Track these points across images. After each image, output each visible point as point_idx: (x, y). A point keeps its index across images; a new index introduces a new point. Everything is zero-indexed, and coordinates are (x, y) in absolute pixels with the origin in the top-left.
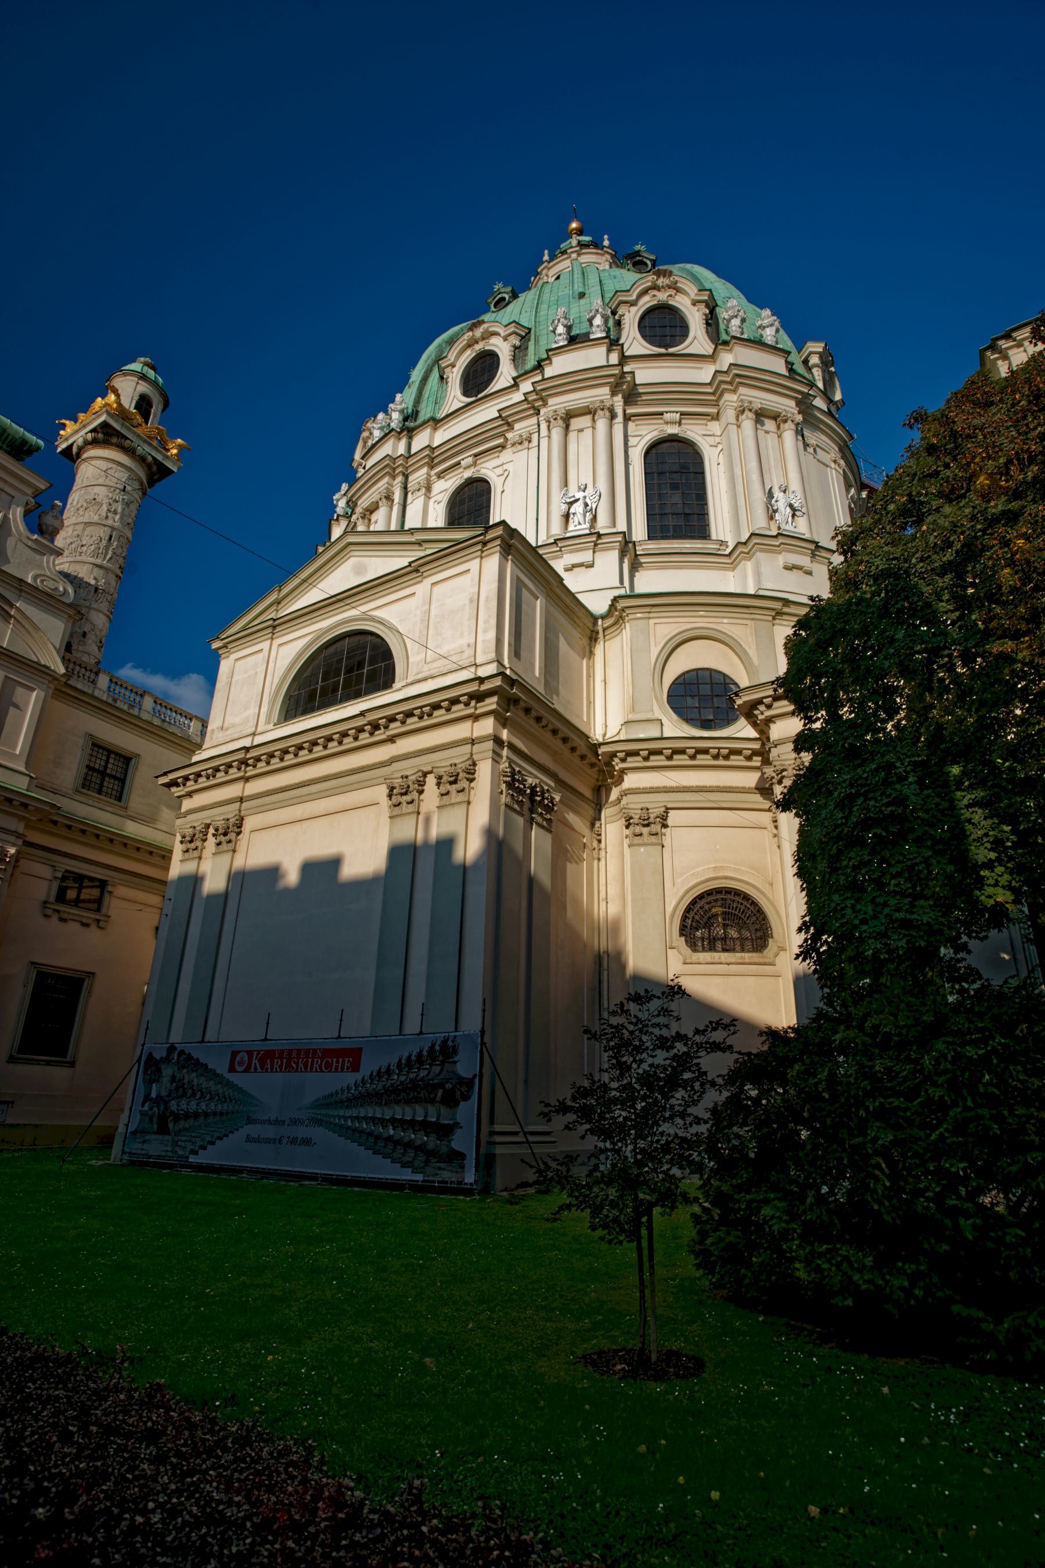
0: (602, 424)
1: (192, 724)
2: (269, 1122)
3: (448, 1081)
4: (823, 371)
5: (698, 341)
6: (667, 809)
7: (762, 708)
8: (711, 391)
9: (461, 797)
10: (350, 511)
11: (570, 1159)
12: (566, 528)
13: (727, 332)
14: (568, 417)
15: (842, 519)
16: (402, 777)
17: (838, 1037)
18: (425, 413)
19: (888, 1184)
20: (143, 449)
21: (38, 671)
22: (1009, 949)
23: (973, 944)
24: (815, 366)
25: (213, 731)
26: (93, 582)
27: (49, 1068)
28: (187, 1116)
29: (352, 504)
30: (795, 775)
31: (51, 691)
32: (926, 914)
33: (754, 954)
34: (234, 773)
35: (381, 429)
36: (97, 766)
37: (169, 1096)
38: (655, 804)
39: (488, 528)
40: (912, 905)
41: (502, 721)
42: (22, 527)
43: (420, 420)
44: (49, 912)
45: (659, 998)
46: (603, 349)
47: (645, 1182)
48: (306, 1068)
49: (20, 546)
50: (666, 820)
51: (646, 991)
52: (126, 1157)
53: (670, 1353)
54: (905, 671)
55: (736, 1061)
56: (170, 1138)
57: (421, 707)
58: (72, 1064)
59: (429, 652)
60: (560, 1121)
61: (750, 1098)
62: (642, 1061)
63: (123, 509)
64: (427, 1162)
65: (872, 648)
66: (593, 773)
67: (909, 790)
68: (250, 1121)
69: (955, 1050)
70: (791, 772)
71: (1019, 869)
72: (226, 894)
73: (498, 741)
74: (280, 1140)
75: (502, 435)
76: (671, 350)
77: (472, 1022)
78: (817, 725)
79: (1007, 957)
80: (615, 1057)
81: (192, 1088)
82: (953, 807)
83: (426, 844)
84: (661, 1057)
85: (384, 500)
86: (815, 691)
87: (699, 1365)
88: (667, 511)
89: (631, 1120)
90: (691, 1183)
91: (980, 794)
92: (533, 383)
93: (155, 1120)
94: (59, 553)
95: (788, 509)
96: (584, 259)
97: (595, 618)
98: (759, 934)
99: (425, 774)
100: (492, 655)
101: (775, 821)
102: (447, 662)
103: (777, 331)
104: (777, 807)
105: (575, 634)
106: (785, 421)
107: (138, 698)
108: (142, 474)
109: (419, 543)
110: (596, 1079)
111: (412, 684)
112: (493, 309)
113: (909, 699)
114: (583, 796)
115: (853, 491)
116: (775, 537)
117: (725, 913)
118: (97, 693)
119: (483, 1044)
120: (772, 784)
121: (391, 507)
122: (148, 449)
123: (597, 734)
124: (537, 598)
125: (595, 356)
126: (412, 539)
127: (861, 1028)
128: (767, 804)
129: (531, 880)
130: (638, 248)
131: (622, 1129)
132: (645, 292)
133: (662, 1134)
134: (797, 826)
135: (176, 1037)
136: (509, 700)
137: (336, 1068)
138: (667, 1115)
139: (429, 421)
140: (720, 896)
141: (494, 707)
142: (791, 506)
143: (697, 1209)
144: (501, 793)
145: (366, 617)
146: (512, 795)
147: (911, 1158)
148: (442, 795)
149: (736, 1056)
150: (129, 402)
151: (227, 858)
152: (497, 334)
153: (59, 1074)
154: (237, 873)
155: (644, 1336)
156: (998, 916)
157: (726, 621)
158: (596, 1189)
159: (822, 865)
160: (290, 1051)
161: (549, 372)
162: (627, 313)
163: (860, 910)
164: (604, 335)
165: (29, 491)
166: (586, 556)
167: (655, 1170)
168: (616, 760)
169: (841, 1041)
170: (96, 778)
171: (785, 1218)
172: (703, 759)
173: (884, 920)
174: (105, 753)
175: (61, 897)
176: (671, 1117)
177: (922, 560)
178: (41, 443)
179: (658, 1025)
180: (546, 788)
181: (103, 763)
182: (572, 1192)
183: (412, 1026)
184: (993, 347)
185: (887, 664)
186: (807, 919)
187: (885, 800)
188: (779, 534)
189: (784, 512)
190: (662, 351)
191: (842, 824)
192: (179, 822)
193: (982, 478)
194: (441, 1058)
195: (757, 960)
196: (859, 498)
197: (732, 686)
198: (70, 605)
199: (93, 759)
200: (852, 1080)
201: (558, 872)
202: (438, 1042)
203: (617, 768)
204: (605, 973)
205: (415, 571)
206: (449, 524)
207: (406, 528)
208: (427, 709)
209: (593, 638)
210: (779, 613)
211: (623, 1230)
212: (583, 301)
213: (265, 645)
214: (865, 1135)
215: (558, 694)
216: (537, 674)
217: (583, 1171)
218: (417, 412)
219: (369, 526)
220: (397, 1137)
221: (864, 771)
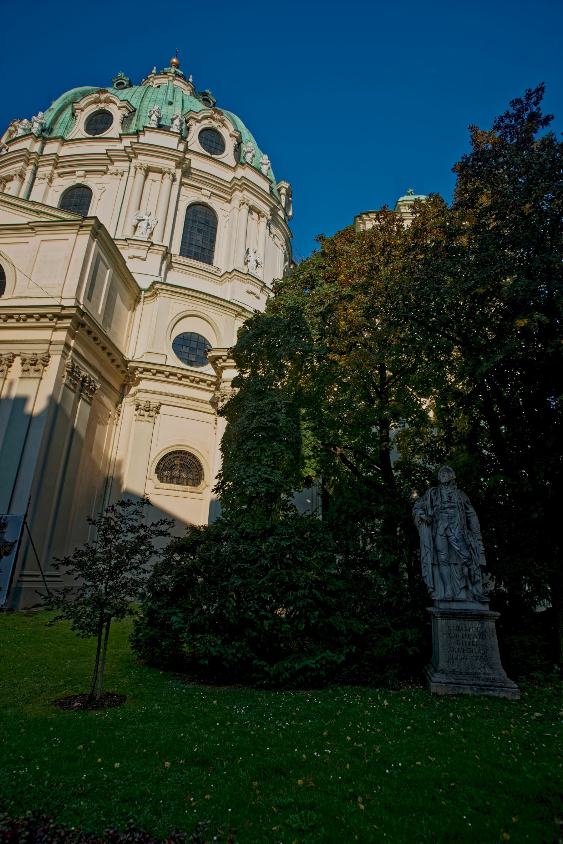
4: (286, 199)
5: (228, 156)
6: (161, 404)
7: (221, 361)
8: (230, 186)
9: (36, 375)
11: (67, 590)
12: (134, 234)
13: (244, 159)
15: (279, 275)
17: (224, 532)
19: (235, 605)
22: (311, 497)
23: (296, 494)
24: (283, 194)
30: (230, 398)
32: (277, 477)
33: (193, 487)
38: (155, 400)
39: (85, 218)
40: (272, 472)
43: (53, 135)
45: (135, 505)
46: (176, 140)
47: (110, 604)
50: (159, 410)
51: (129, 500)
53: (108, 694)
54: (292, 358)
55: (172, 541)
57: (19, 314)
60: (64, 569)
61: (176, 561)
62: (118, 538)
65: (279, 343)
66: (123, 376)
67: (281, 416)
69: (276, 542)
70: (228, 397)
71: (322, 461)
73: (67, 346)
75: (106, 165)
76: (213, 156)
78: (246, 376)
79: (309, 501)
80: (104, 535)
82: (299, 428)
83: (7, 398)
84: (130, 537)
85: (18, 177)
86: (248, 358)
87: (123, 698)
88: (193, 243)
89: (107, 570)
90: (135, 603)
91: (312, 425)
92: (131, 142)
95: (255, 262)
96: (176, 83)
97: (140, 290)
98: (197, 477)
99: (14, 356)
100: (73, 294)
101: (216, 420)
103: (269, 169)
104: (218, 414)
105: (127, 296)
106: (263, 217)
109: (38, 212)
110: (90, 546)
113: (291, 373)
115: (287, 263)
116: (246, 274)
117: (181, 464)
119: (25, 522)
120: (218, 401)
121: (22, 183)
123: (128, 356)
124: (108, 269)
125: (171, 142)
127: (236, 529)
128: (213, 411)
129: (73, 431)
130: (207, 91)
131: (102, 575)
132: (206, 118)
133: (123, 578)
134: (226, 425)
136: (79, 323)
138: (128, 568)
139: (59, 138)
140: (180, 455)
141: (69, 325)
142: (256, 261)
143: (137, 619)
144: (64, 377)
146: (70, 380)
147: (248, 592)
148: (24, 371)
149: (173, 539)
152: (116, 104)
155: (94, 687)
156: (308, 482)
157: (211, 311)
158: (79, 608)
159: (234, 446)
161: (142, 139)
162: (194, 125)
163: (247, 471)
164: (178, 131)
167: (116, 597)
168: (137, 372)
169: (225, 536)
171: (182, 622)
172: (185, 381)
173: (257, 478)
176: (130, 569)
177: (310, 307)
179: (132, 519)
180: (92, 379)
182: (65, 609)
184: (360, 217)
185: (284, 353)
186: (221, 472)
187: (269, 419)
188: (248, 274)
189: (252, 264)
190: (209, 154)
191: (247, 427)
193: (342, 276)
195: (193, 490)
196: (290, 268)
197: (208, 346)
200: (227, 554)
201: (91, 428)
203: (137, 376)
204: (109, 488)
206: (60, 207)
207: (30, 200)
209: (137, 301)
210: (239, 314)
211: (92, 630)
212: (170, 107)
214: (228, 581)
215: (110, 327)
216: (99, 312)
217: (75, 597)
219: (3, 189)
221: (262, 403)
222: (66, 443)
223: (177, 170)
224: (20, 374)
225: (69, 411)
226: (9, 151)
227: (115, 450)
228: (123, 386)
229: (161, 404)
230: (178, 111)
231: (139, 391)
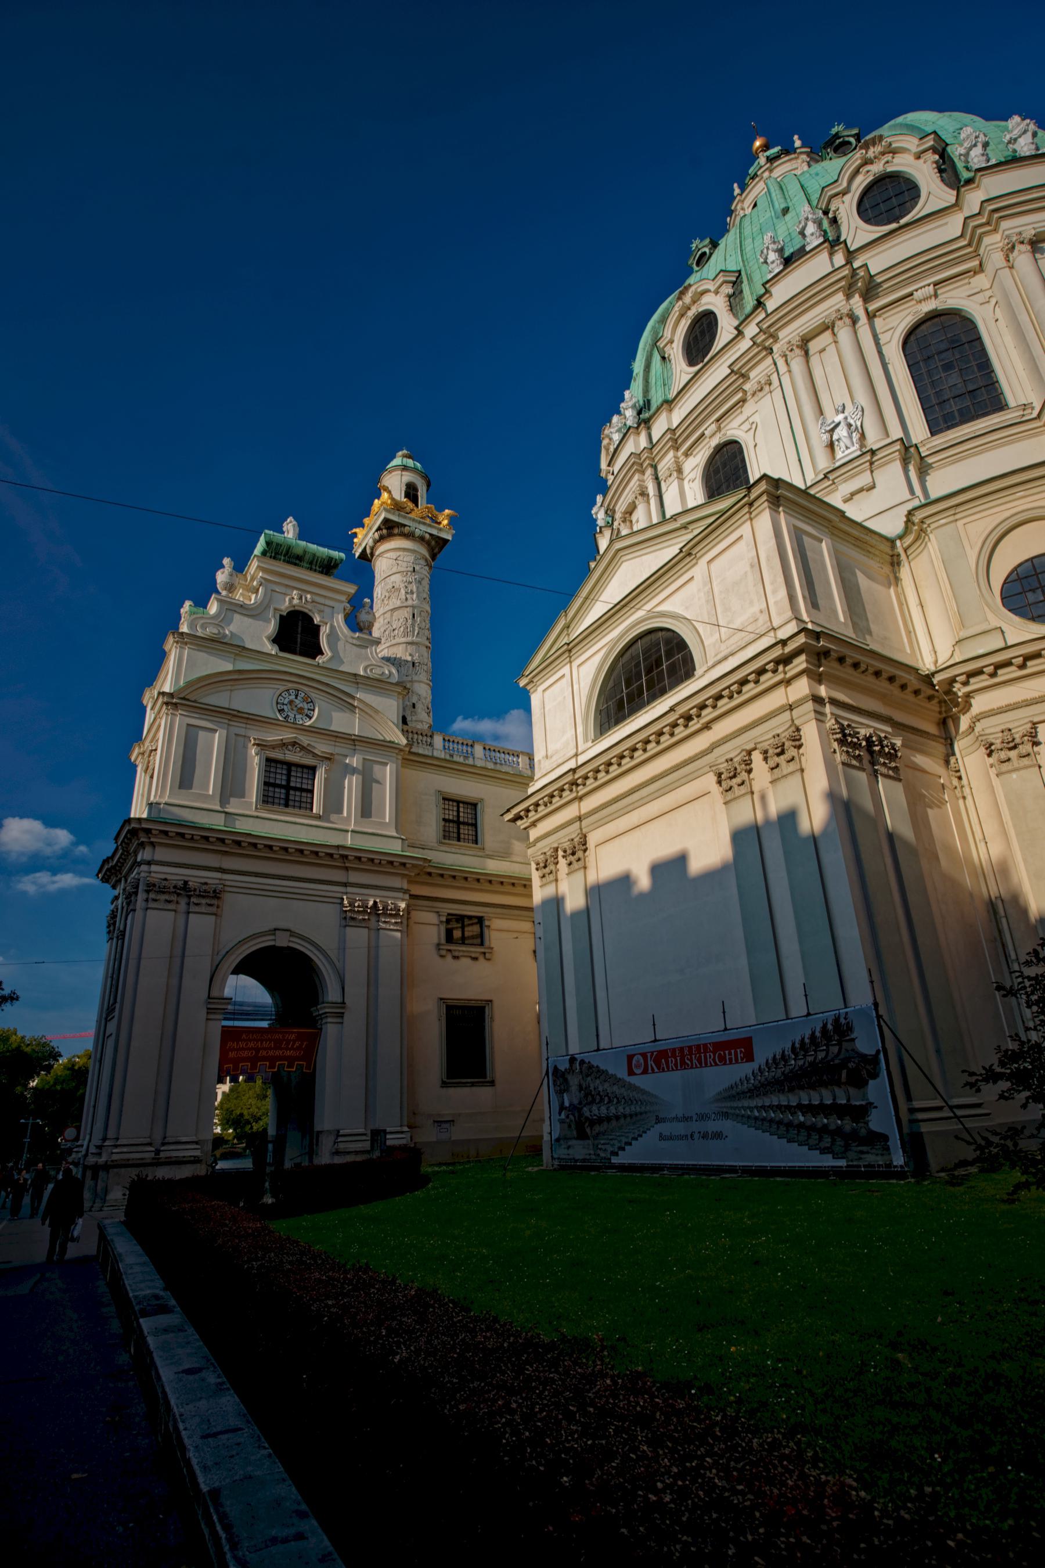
0: (844, 333)
1: (520, 760)
2: (676, 1119)
3: (848, 1059)
6: (1034, 725)
9: (792, 766)
10: (610, 520)
14: (804, 343)
16: (727, 761)
18: (656, 400)
20: (421, 529)
21: (387, 746)
25: (540, 761)
26: (409, 658)
27: (474, 1089)
28: (600, 1120)
29: (610, 512)
31: (400, 762)
34: (567, 795)
35: (619, 431)
36: (451, 817)
37: (580, 1103)
38: (1018, 722)
39: (750, 488)
41: (818, 678)
42: (345, 629)
43: (654, 407)
44: (443, 953)
46: (824, 255)
48: (700, 1063)
49: (348, 646)
50: (1036, 736)
52: (556, 1163)
56: (590, 1142)
57: (729, 687)
58: (492, 1083)
59: (723, 630)
63: (418, 588)
64: (847, 1148)
66: (934, 705)
68: (659, 1120)
72: (588, 909)
73: (817, 700)
74: (692, 1136)
75: (740, 389)
76: (903, 221)
77: (861, 996)
81: (599, 1094)
83: (767, 822)
85: (639, 497)
88: (946, 398)
92: (757, 324)
93: (573, 1126)
94: (377, 642)
96: (776, 173)
97: (892, 542)
99: (749, 753)
100: (789, 614)
102: (743, 634)
105: (873, 564)
107: (469, 749)
108: (424, 551)
109: (685, 527)
111: (713, 666)
112: (695, 268)
114: (928, 733)
118: (436, 754)
119: (879, 1017)
121: (648, 502)
122: (423, 528)
123: (927, 664)
124: (821, 541)
125: (818, 266)
126: (677, 525)
129: (891, 837)
135: (574, 1049)
136: (818, 654)
137: (730, 1059)
139: (662, 405)
141: (804, 666)
144: (835, 752)
145: (653, 615)
146: (847, 752)
148: (772, 769)
150: (399, 495)
151: (580, 875)
152: (707, 291)
153: (483, 1093)
154: (593, 888)
160: (682, 1049)
161: (771, 305)
164: (821, 240)
165: (344, 598)
166: (864, 479)
168: (957, 686)
170: (453, 828)
174: (455, 804)
175: (449, 938)
178: (343, 555)
180: (883, 735)
181: (455, 813)
183: (798, 1008)
190: (894, 226)
192: (530, 851)
194: (836, 1037)
198: (397, 684)
199: (447, 812)
202: (830, 1022)
203: (960, 694)
204: (1004, 920)
205: (687, 554)
206: (709, 497)
207: (668, 516)
208: (735, 687)
209: (895, 562)
212: (788, 217)
213: (566, 670)
215: (870, 633)
216: (842, 619)
218: (649, 401)
219: (632, 528)
220: (808, 1123)
222: (889, 861)
223: (852, 301)
224: (768, 777)
225: (869, 805)
226: (615, 473)
227: (982, 846)
228: (943, 723)
229: (1034, 725)
230: (804, 209)
231: (978, 719)
